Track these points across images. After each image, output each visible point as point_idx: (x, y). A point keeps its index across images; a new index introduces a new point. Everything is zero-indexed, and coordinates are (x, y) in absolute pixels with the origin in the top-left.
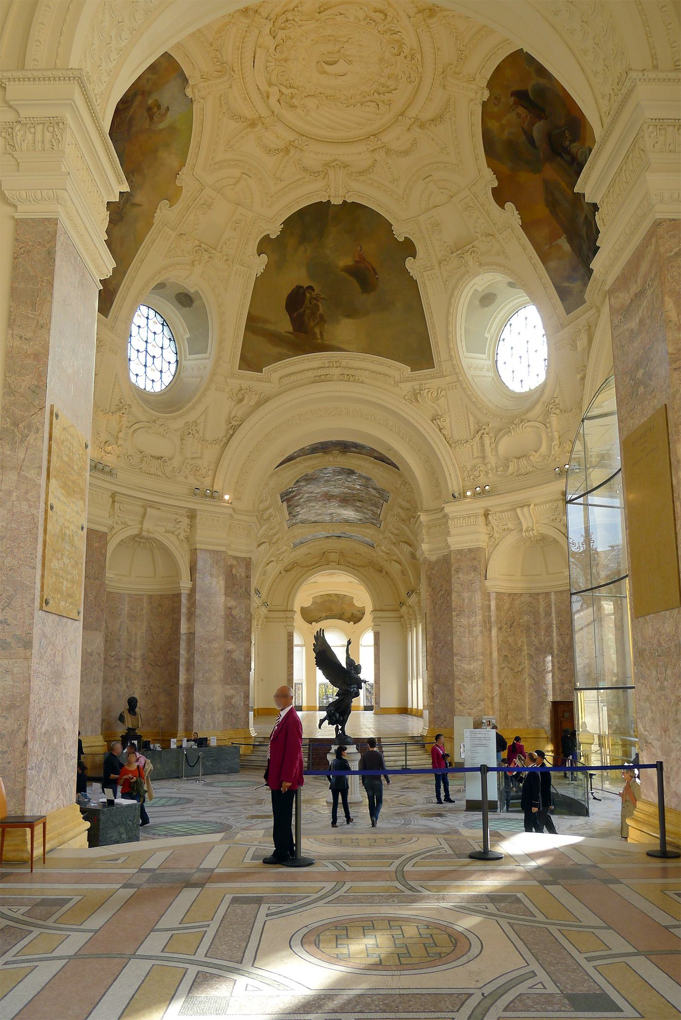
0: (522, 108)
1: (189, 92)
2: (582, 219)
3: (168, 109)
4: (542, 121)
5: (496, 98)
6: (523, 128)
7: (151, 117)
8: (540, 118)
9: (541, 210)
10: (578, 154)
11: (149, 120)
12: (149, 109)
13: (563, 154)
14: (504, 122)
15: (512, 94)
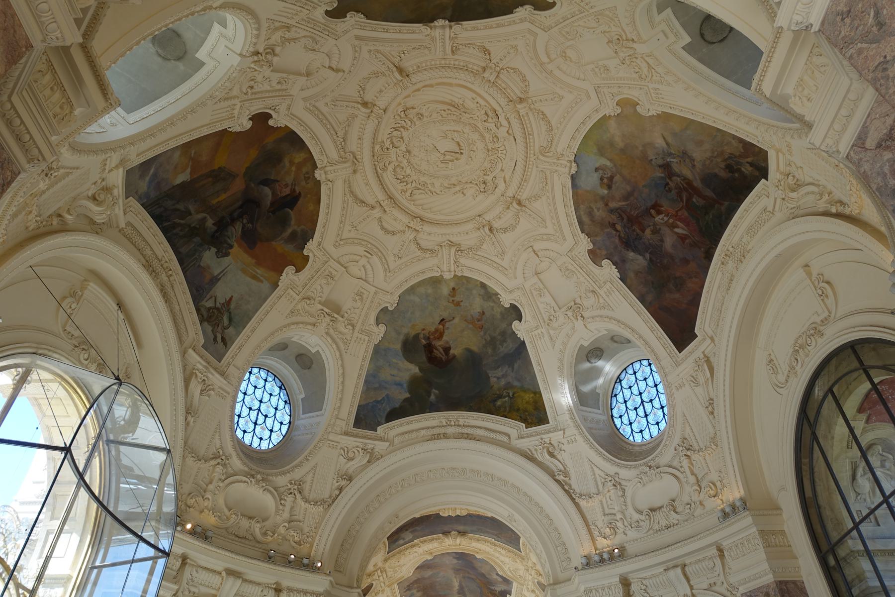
0: (287, 194)
1: (574, 169)
2: (192, 208)
3: (597, 170)
4: (269, 204)
5: (309, 178)
6: (278, 181)
7: (611, 179)
8: (272, 204)
9: (221, 161)
10: (233, 228)
11: (614, 180)
12: (609, 187)
13: (241, 210)
14: (293, 169)
15: (300, 193)
